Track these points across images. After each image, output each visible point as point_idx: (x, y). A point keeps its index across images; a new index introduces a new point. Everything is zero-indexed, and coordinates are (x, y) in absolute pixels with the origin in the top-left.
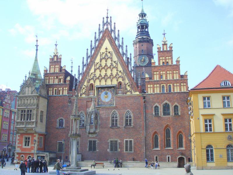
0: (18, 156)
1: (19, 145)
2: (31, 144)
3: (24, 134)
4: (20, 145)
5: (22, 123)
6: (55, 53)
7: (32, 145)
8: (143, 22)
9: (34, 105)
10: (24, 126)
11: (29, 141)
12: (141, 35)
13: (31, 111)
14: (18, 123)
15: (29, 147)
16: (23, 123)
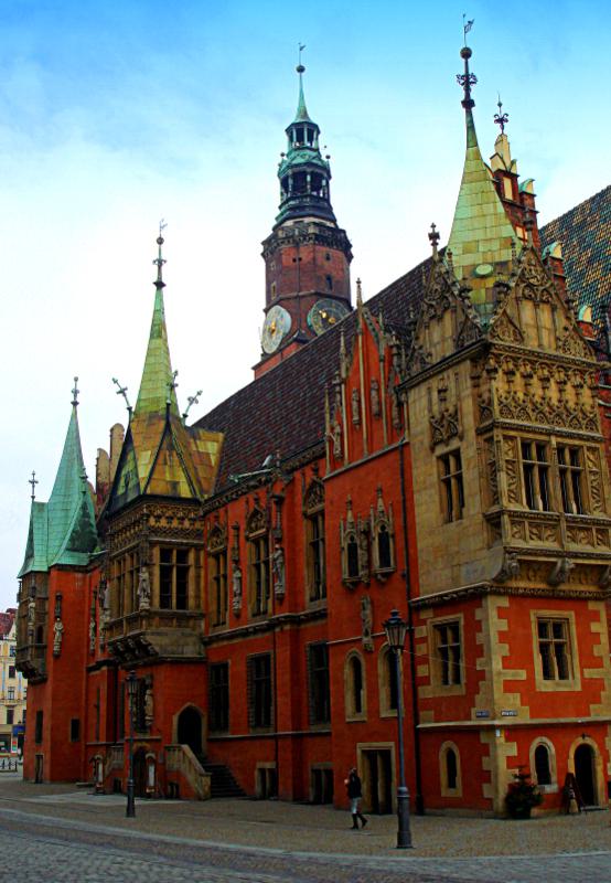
0: (513, 750)
1: (510, 675)
2: (582, 667)
3: (533, 596)
4: (522, 675)
5: (537, 526)
6: (508, 164)
7: (589, 673)
8: (320, 163)
9: (592, 423)
10: (551, 545)
11: (559, 647)
12: (317, 213)
13: (574, 452)
14: (517, 518)
15: (574, 684)
16: (553, 523)
